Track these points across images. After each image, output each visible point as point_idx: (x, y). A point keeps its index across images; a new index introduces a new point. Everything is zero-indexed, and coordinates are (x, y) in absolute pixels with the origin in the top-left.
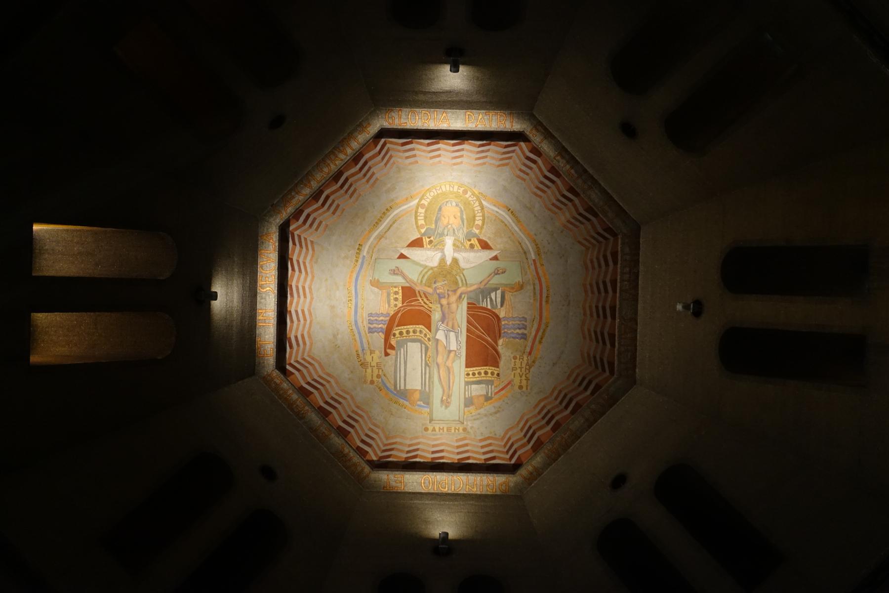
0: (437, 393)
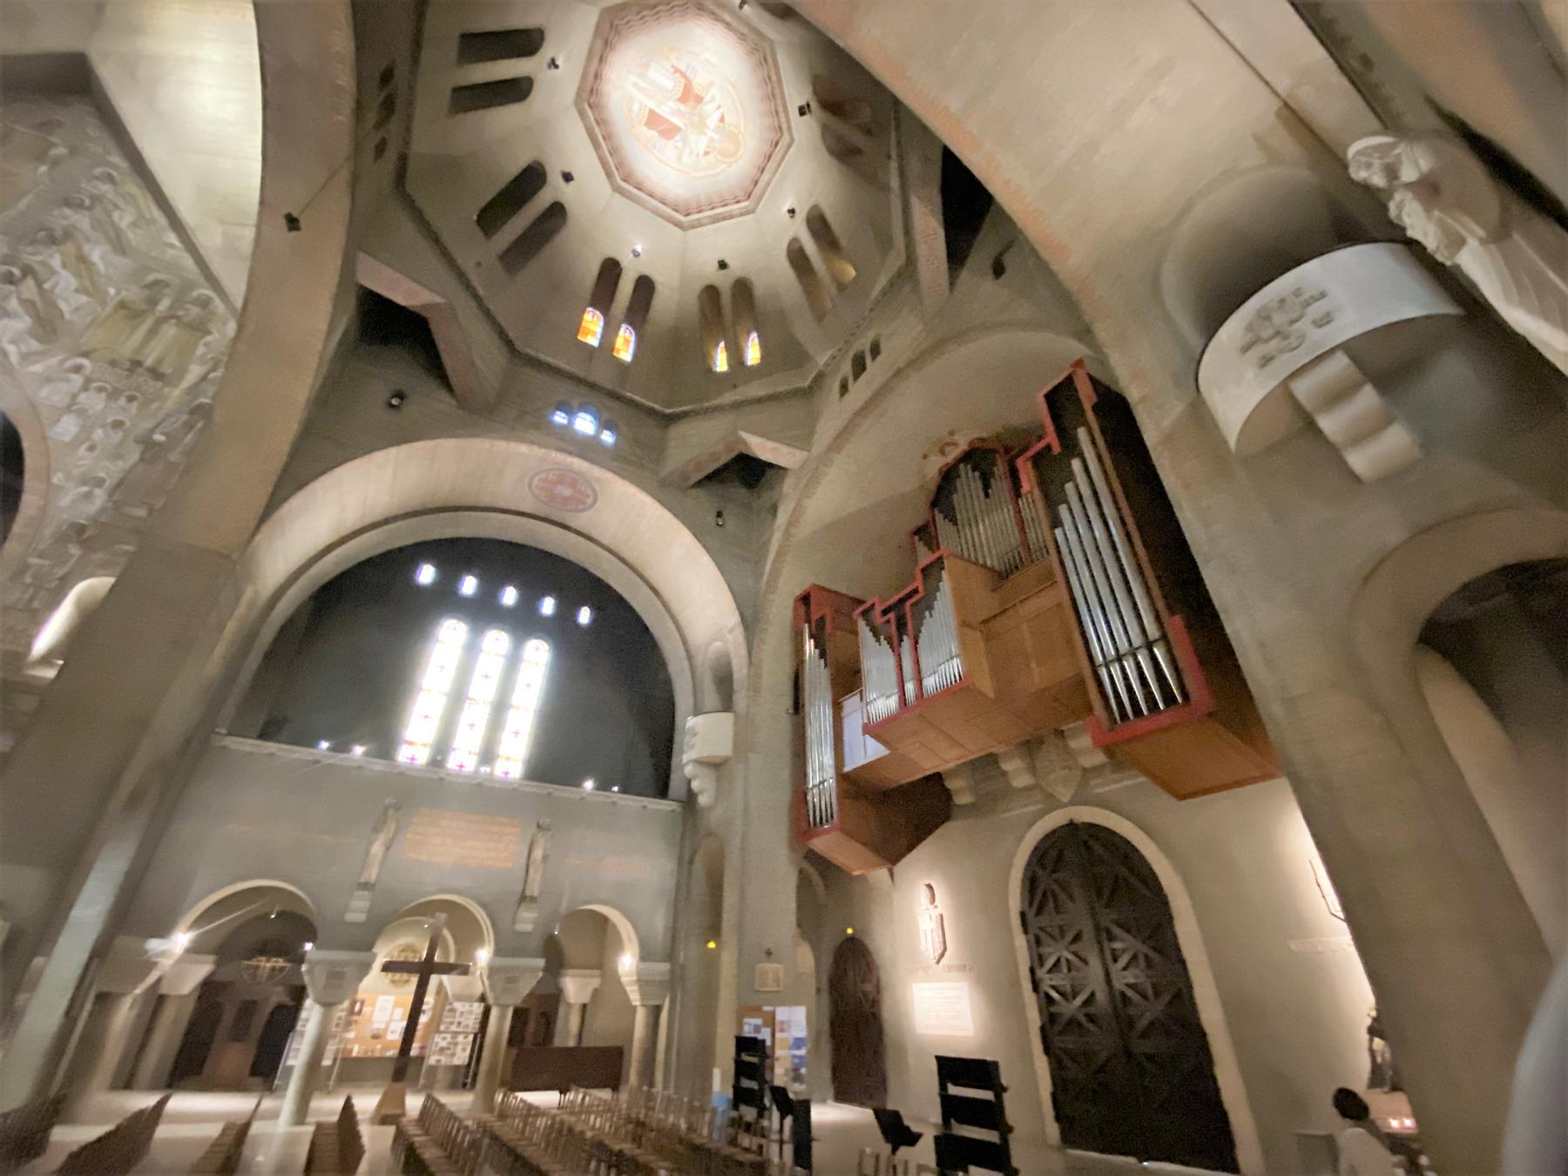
0: (642, 84)
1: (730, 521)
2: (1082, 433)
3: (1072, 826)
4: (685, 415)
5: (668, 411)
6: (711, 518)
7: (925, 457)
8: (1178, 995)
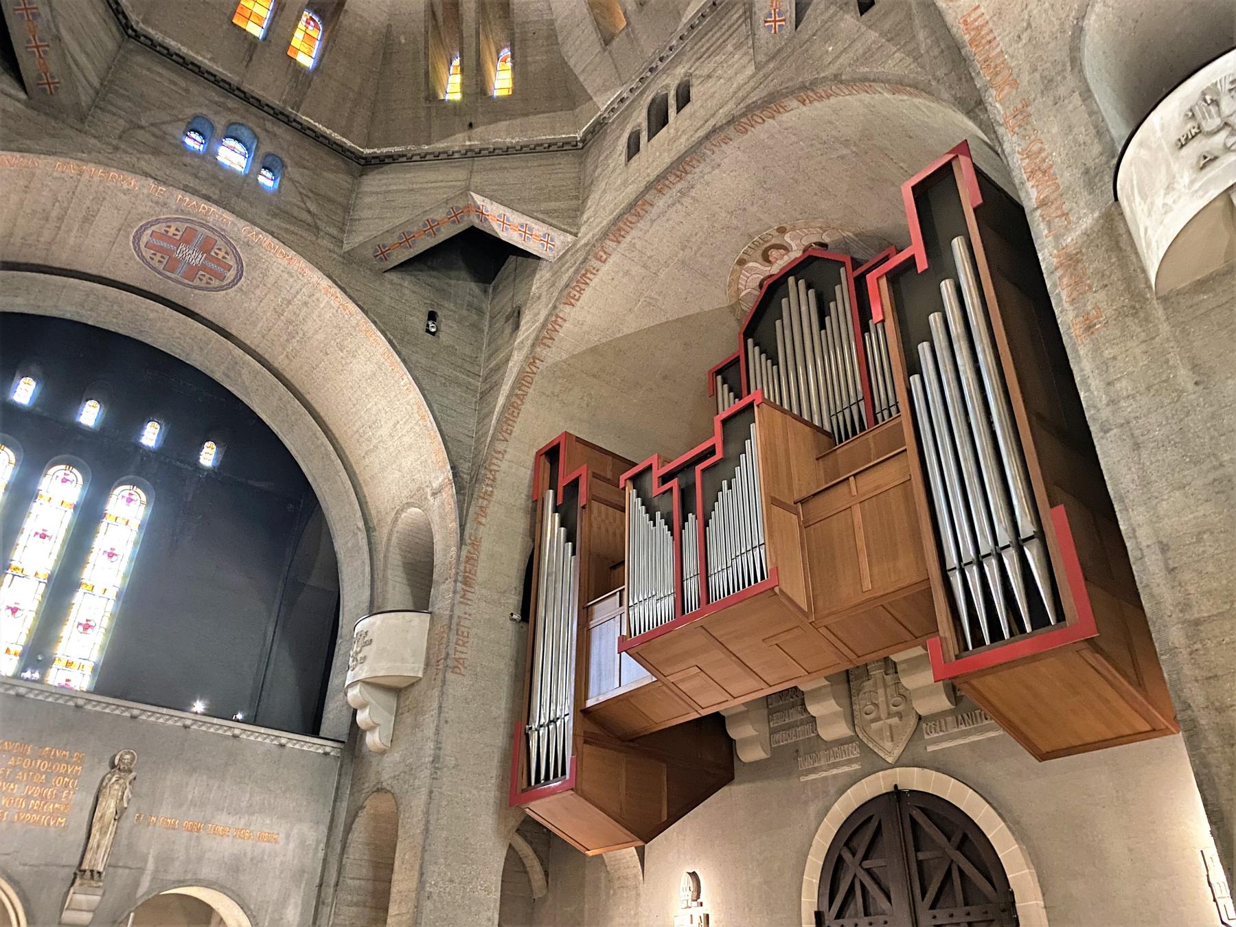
1: (448, 328)
2: (958, 244)
3: (897, 794)
4: (392, 159)
5: (368, 151)
6: (418, 321)
7: (741, 262)
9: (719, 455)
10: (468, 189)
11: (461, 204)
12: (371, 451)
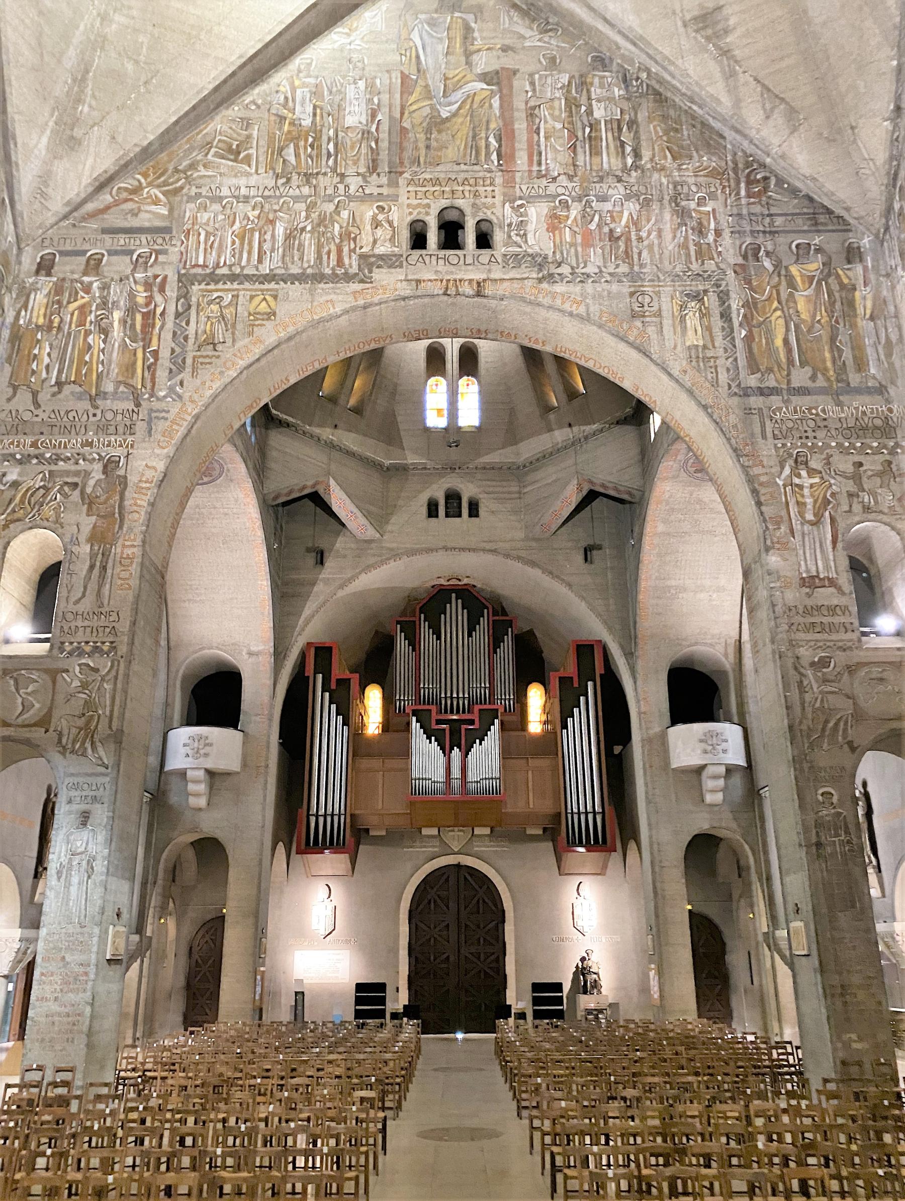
3: (458, 866)
4: (288, 425)
5: (274, 412)
8: (498, 958)
9: (476, 726)
10: (328, 474)
11: (320, 479)
12: (196, 602)
